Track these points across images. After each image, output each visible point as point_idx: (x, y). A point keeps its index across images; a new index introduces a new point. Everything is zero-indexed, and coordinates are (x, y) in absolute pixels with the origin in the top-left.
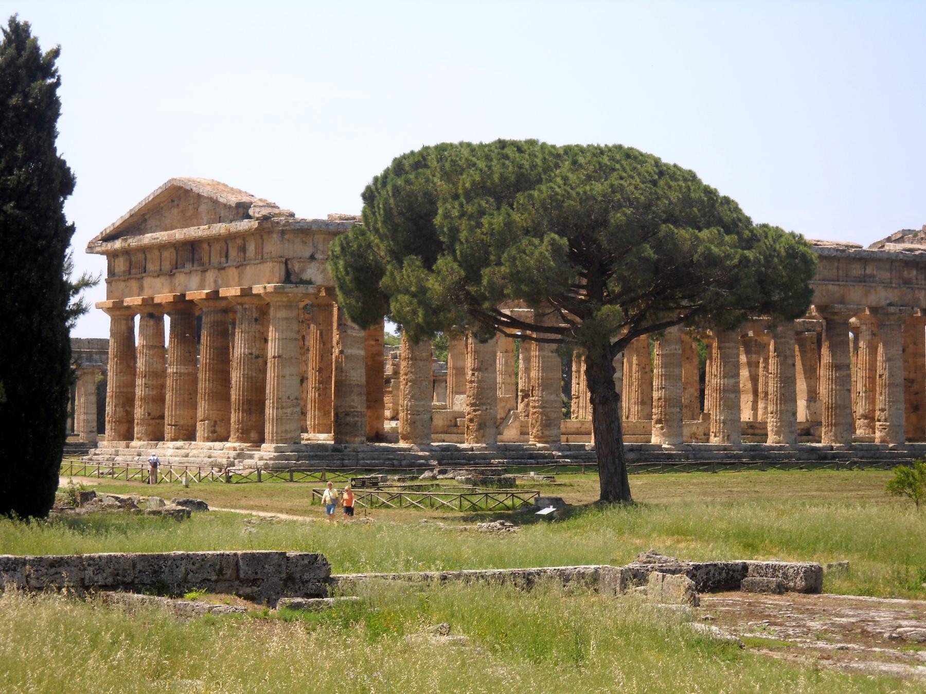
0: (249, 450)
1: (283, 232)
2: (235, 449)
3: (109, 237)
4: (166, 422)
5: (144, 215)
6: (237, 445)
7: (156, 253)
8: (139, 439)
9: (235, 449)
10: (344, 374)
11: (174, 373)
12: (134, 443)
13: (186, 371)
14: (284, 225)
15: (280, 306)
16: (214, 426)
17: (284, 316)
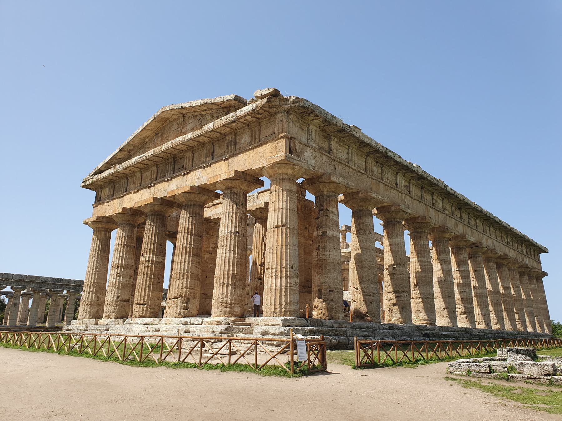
0: (235, 324)
1: (288, 112)
2: (219, 323)
3: (100, 171)
4: (135, 302)
5: (130, 151)
6: (221, 319)
7: (138, 175)
8: (108, 317)
9: (219, 323)
10: (328, 253)
11: (146, 261)
12: (104, 321)
13: (157, 260)
14: (294, 102)
15: (283, 179)
16: (187, 303)
17: (288, 188)
